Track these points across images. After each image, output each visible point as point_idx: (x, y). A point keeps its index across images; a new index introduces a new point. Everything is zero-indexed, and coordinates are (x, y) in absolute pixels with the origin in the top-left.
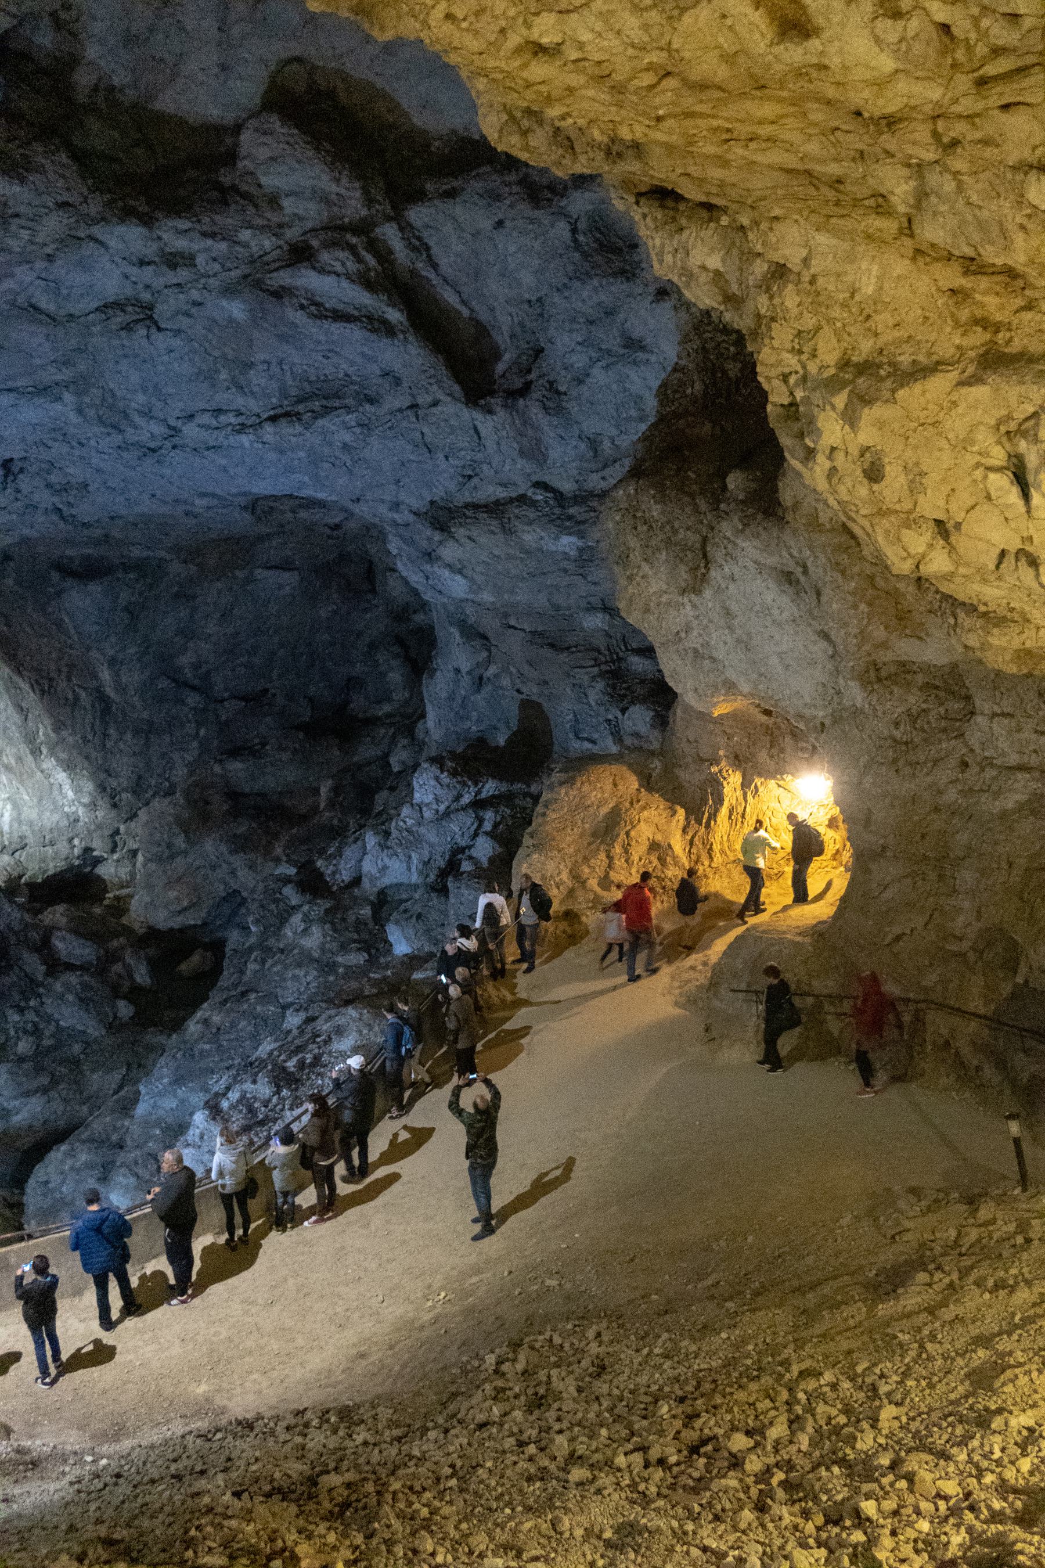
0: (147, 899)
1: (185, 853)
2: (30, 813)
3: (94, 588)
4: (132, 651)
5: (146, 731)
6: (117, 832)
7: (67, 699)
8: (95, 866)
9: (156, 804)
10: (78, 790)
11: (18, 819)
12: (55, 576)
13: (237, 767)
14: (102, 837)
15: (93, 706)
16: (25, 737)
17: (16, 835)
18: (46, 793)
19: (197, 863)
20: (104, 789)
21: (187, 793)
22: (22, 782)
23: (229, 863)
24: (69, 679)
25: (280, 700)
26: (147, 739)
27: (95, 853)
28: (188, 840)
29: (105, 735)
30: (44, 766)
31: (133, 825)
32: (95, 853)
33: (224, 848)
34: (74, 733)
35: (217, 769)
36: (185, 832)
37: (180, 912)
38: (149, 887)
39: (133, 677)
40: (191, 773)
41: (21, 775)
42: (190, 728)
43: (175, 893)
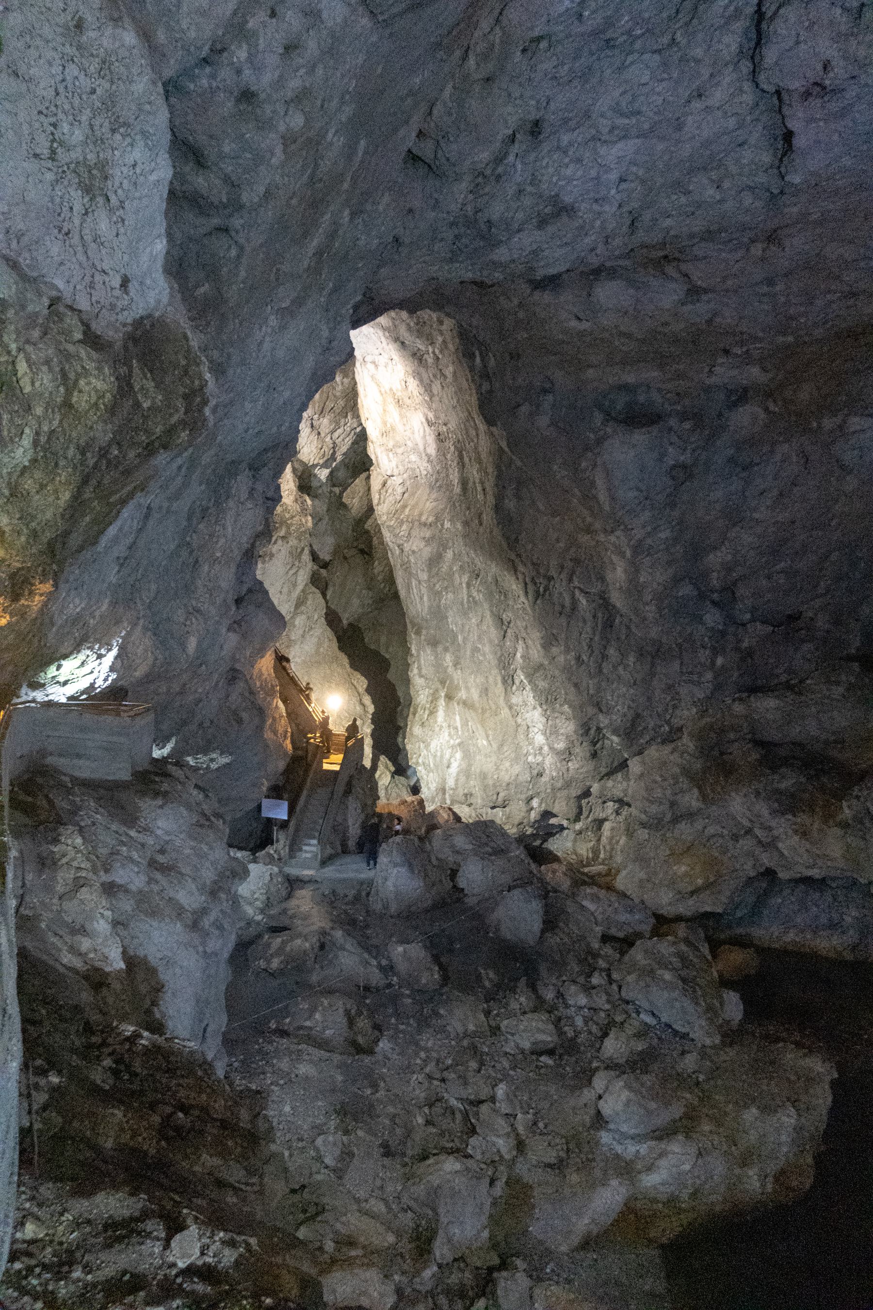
0: (642, 875)
1: (690, 816)
2: (484, 763)
3: (640, 437)
4: (663, 535)
5: (653, 654)
6: (587, 794)
7: (563, 606)
8: (545, 841)
9: (653, 752)
10: (551, 732)
11: (466, 773)
12: (598, 418)
13: (768, 706)
14: (568, 798)
15: (594, 617)
16: (500, 660)
17: (461, 791)
18: (510, 736)
19: (711, 830)
20: (587, 732)
21: (699, 736)
22: (482, 722)
23: (770, 829)
24: (570, 580)
25: (822, 623)
26: (653, 665)
27: (553, 821)
28: (704, 797)
29: (604, 657)
30: (514, 700)
31: (610, 783)
32: (553, 821)
33: (763, 809)
34: (567, 650)
35: (738, 708)
36: (699, 788)
37: (692, 893)
38: (641, 859)
39: (654, 577)
40: (703, 713)
41: (484, 711)
42: (703, 655)
43: (683, 868)
